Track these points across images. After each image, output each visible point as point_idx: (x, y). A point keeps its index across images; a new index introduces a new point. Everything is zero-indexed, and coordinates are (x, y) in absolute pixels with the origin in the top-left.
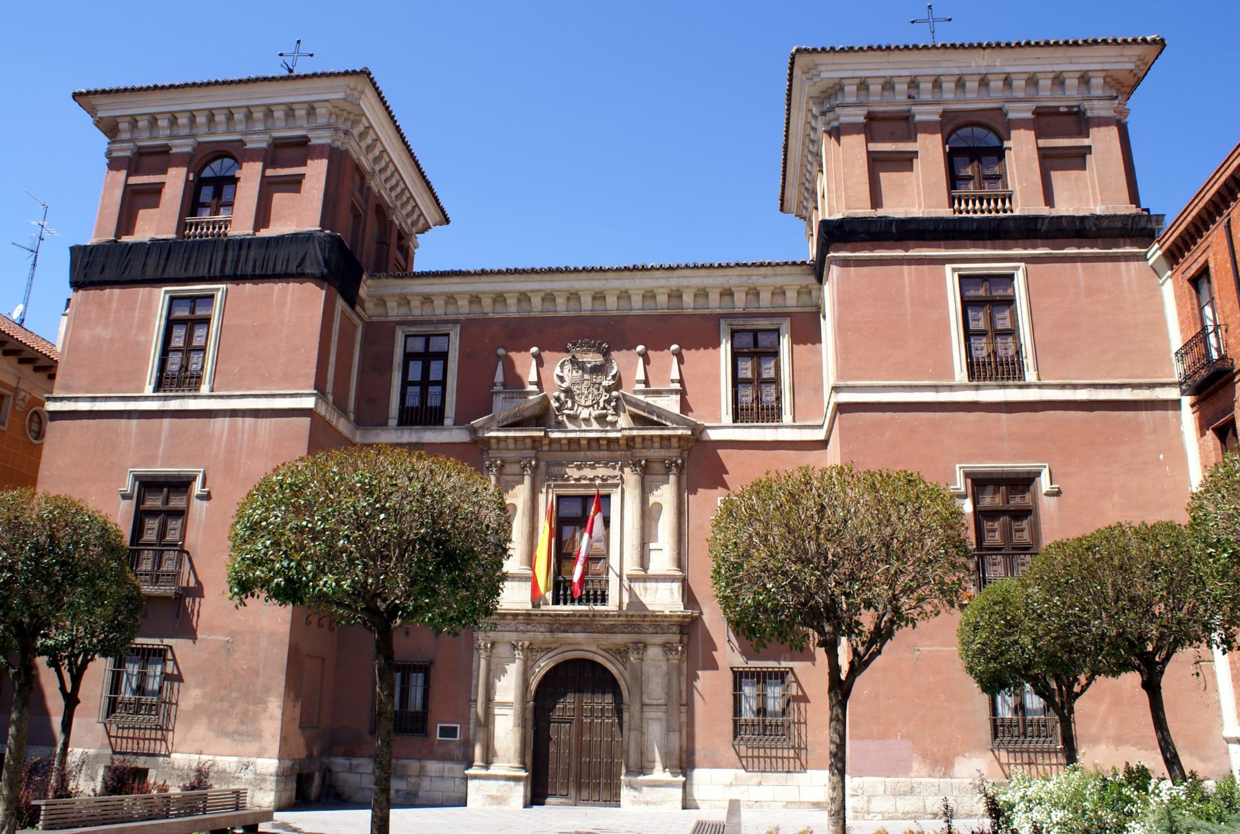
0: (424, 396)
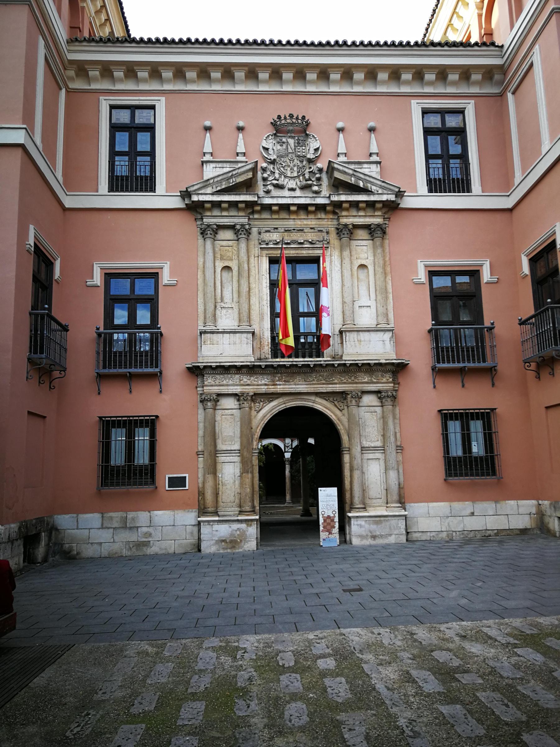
0: (133, 165)
